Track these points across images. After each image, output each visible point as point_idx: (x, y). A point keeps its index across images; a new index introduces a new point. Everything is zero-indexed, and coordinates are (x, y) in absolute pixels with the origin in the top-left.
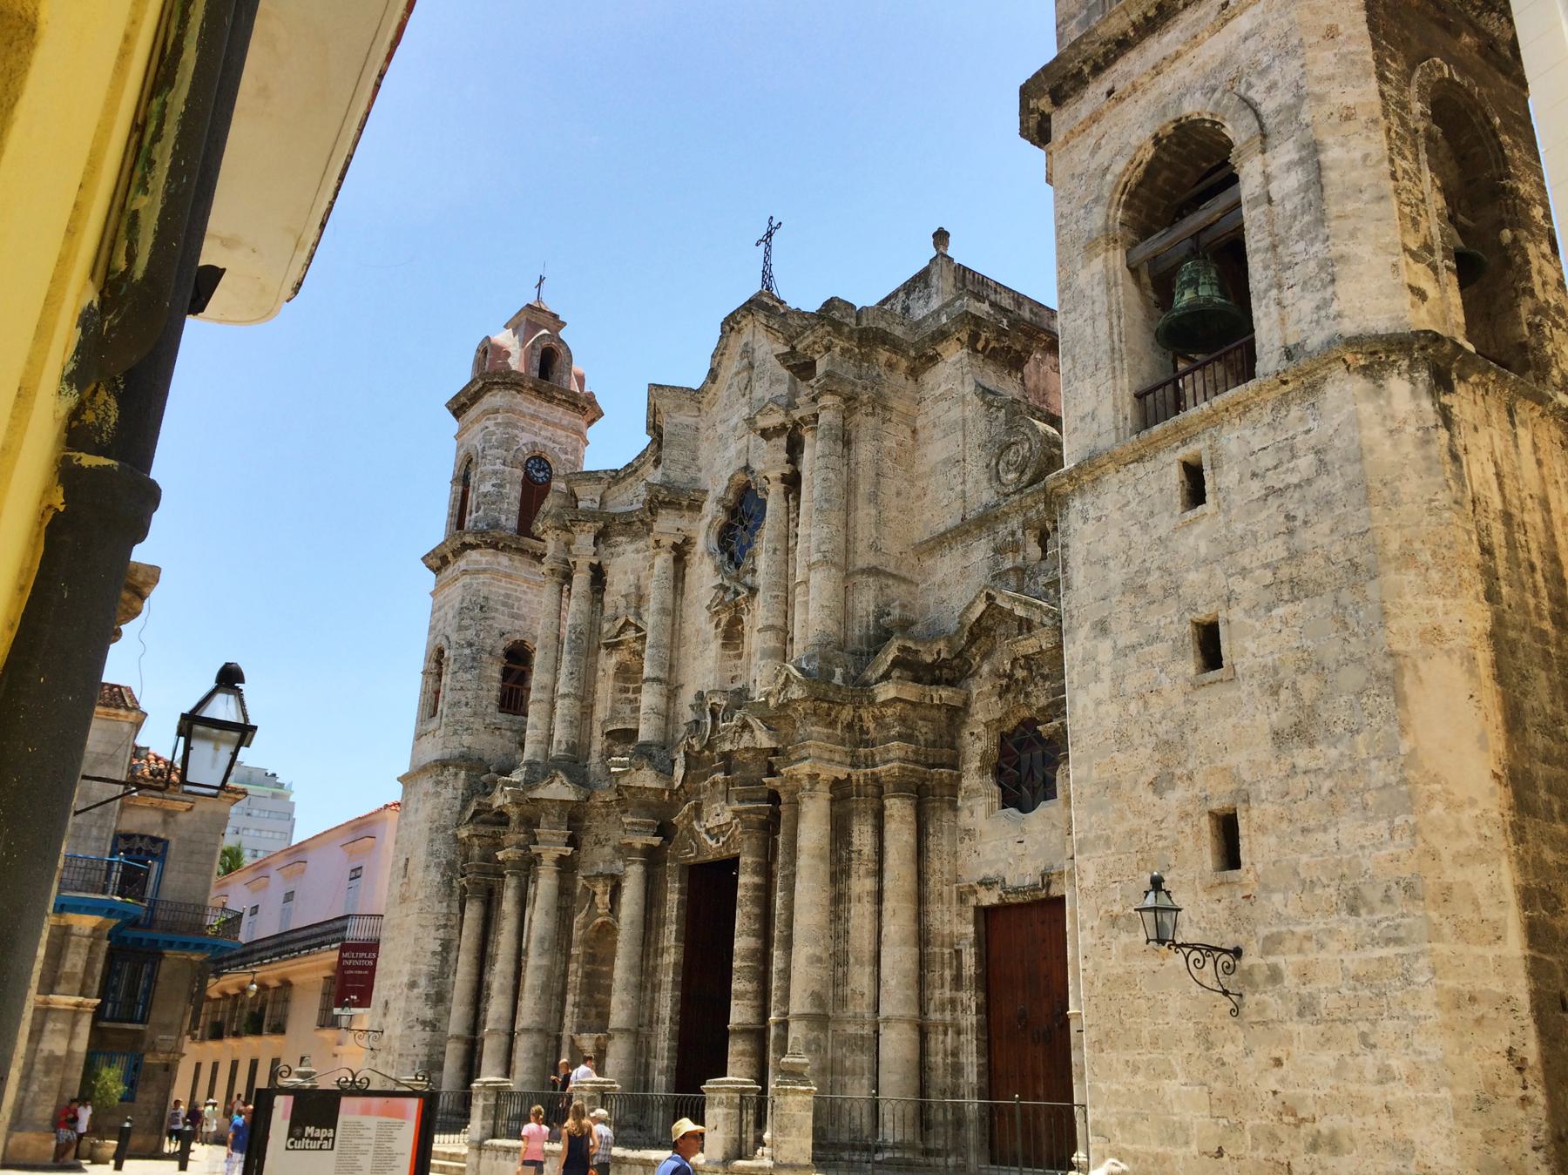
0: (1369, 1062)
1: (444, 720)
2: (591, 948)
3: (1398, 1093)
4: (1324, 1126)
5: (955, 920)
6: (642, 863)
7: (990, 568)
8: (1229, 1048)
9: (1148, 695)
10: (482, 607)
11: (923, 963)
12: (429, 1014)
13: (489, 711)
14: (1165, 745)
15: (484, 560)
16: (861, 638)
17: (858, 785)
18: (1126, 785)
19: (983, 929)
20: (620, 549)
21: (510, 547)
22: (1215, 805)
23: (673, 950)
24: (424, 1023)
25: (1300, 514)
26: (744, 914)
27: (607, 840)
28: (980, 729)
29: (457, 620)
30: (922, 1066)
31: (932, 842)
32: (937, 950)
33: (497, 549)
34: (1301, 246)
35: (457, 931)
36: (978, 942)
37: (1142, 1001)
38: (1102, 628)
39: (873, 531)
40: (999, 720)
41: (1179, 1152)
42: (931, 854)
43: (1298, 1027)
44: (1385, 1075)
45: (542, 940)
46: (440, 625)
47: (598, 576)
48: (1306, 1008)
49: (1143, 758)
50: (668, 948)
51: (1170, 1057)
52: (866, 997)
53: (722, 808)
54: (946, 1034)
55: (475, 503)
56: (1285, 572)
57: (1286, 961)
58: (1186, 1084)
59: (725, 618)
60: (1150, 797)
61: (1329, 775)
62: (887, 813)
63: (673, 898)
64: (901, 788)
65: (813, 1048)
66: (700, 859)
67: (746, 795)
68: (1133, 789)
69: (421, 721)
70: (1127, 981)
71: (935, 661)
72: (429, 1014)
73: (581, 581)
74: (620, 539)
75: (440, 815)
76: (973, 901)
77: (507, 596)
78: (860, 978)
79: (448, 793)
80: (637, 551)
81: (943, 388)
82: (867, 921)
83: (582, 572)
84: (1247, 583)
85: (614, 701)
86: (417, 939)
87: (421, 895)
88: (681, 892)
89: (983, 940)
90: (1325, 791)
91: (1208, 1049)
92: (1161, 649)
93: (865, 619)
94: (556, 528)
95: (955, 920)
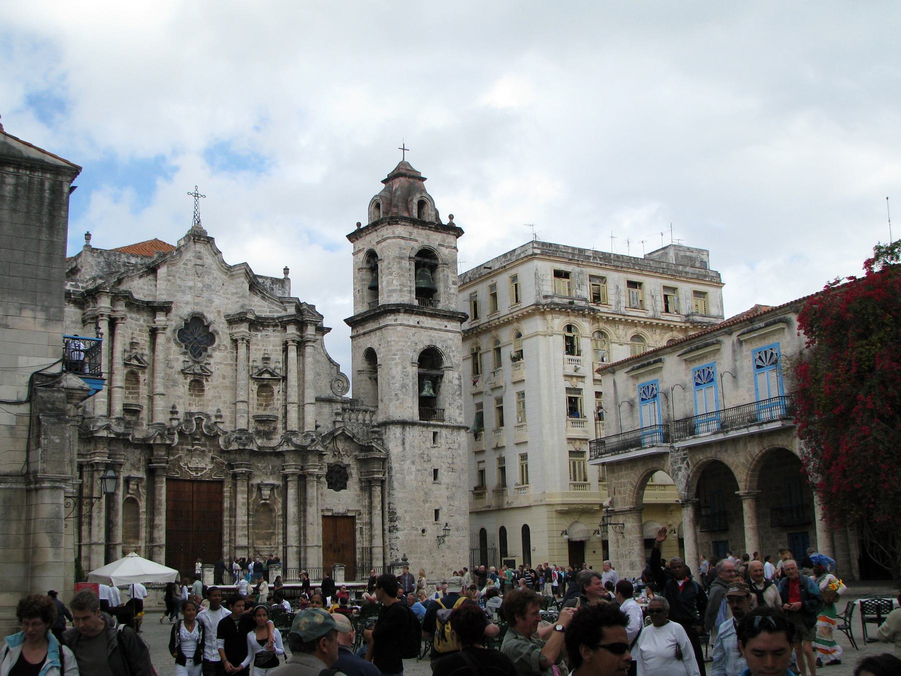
4: (450, 567)
14: (426, 493)
34: (457, 398)
43: (447, 550)
48: (449, 547)
53: (200, 461)
56: (452, 466)
70: (416, 541)
92: (426, 473)
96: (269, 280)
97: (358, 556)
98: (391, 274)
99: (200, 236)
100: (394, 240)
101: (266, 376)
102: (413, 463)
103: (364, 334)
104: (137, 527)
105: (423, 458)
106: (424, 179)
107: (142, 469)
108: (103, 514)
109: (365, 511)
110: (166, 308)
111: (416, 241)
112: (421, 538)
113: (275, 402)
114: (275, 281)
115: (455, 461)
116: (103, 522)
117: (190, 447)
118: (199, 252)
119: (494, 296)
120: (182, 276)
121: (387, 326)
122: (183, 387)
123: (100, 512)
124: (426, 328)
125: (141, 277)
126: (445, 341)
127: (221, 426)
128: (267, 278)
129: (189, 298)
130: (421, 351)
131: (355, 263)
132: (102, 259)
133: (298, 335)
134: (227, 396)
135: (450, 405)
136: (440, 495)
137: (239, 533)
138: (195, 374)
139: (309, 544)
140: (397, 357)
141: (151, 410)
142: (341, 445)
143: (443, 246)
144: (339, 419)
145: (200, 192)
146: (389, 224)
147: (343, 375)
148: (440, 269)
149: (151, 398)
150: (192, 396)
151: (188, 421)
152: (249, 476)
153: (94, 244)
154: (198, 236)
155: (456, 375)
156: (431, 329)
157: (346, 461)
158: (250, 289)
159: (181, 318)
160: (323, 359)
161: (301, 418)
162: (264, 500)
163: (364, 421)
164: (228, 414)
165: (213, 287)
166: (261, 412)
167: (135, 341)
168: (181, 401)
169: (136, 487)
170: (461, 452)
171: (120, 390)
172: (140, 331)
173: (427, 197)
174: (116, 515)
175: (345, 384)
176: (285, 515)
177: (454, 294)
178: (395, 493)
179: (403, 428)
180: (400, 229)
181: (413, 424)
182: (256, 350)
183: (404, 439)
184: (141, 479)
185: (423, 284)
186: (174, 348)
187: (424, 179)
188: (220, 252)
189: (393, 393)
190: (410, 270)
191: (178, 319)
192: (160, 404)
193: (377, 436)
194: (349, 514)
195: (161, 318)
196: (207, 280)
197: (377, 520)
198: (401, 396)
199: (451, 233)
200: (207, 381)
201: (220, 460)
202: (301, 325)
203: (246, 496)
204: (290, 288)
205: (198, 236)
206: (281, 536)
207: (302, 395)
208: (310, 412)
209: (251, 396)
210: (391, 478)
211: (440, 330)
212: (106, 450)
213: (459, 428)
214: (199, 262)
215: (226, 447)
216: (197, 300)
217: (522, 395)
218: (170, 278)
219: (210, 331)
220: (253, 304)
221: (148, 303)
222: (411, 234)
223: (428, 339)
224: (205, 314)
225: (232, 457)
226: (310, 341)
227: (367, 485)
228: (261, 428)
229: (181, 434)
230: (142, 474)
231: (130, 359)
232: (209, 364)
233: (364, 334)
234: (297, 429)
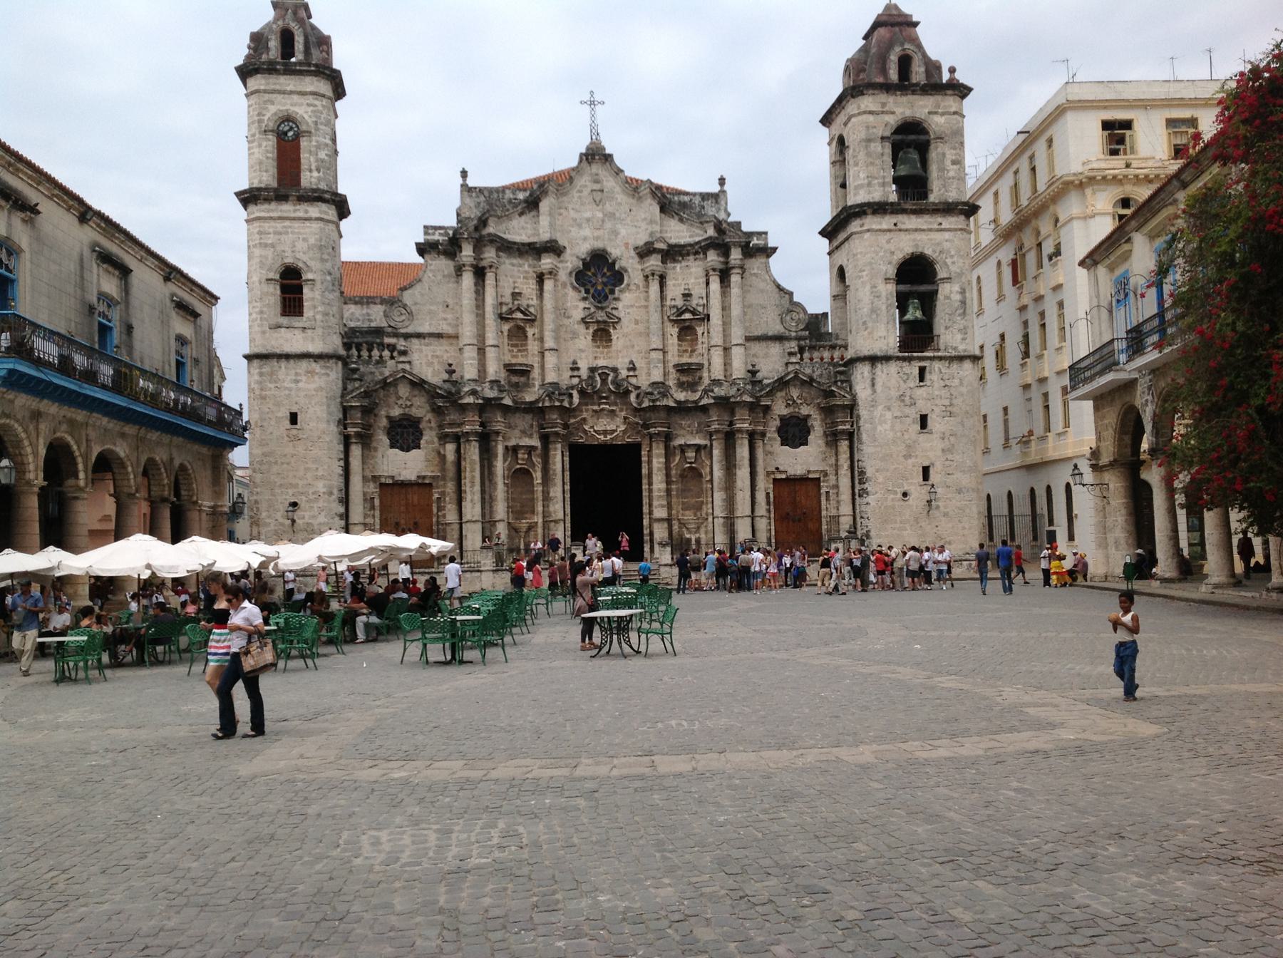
0: (960, 525)
3: (966, 532)
10: (333, 248)
14: (909, 446)
15: (330, 212)
18: (894, 456)
20: (502, 260)
25: (955, 394)
44: (964, 528)
48: (946, 515)
49: (902, 448)
56: (948, 409)
60: (902, 459)
63: (567, 459)
70: (893, 507)
72: (342, 510)
74: (501, 254)
80: (513, 265)
81: (755, 271)
92: (909, 420)
96: (697, 197)
97: (824, 527)
98: (856, 164)
99: (593, 155)
100: (860, 118)
101: (687, 316)
102: (889, 409)
103: (837, 248)
104: (532, 500)
105: (903, 401)
106: (916, 24)
107: (536, 436)
108: (477, 488)
109: (830, 471)
110: (553, 248)
111: (893, 113)
112: (902, 503)
113: (700, 346)
114: (705, 196)
115: (954, 402)
116: (477, 497)
117: (596, 408)
118: (597, 175)
119: (1033, 169)
120: (577, 207)
121: (852, 234)
122: (584, 339)
123: (472, 486)
124: (906, 230)
125: (521, 214)
126: (938, 244)
127: (633, 381)
128: (694, 194)
129: (587, 232)
130: (901, 261)
131: (831, 156)
132: (482, 198)
133: (723, 263)
134: (641, 344)
135: (946, 328)
136: (930, 448)
137: (655, 503)
138: (598, 322)
139: (738, 513)
140: (864, 273)
141: (543, 367)
142: (795, 393)
143: (936, 113)
144: (794, 360)
145: (597, 98)
146: (853, 97)
147: (798, 305)
148: (932, 147)
149: (542, 354)
150: (598, 347)
151: (589, 377)
152: (668, 437)
153: (471, 182)
154: (596, 155)
155: (956, 288)
156: (916, 230)
157: (805, 410)
158: (663, 210)
159: (577, 257)
160: (771, 287)
161: (727, 364)
162: (691, 463)
163: (832, 358)
164: (643, 365)
165: (617, 215)
166: (685, 360)
167: (517, 291)
168: (583, 355)
169: (526, 456)
170: (964, 390)
171: (493, 349)
172: (524, 278)
173: (912, 48)
174: (495, 489)
175: (802, 315)
176: (711, 481)
177: (953, 178)
178: (864, 447)
179: (873, 365)
180: (868, 102)
181: (887, 359)
182: (674, 285)
183: (873, 379)
184: (532, 448)
185: (903, 170)
186: (571, 293)
187: (916, 24)
188: (622, 171)
189: (861, 322)
190: (882, 155)
191: (575, 259)
192: (551, 359)
193: (842, 378)
194: (811, 476)
195: (547, 262)
196: (609, 207)
197: (845, 482)
198: (870, 325)
199: (949, 92)
200: (615, 328)
201: (632, 419)
202: (724, 250)
203: (663, 460)
204: (726, 204)
205: (596, 155)
206: (710, 506)
207: (726, 334)
208: (738, 356)
209: (670, 342)
210: (859, 430)
211: (930, 230)
212: (476, 418)
213: (961, 358)
214: (597, 187)
215: (640, 404)
216: (597, 233)
217: (1061, 305)
218: (562, 211)
219: (617, 267)
220: (669, 229)
221: (530, 244)
222: (884, 105)
223: (911, 243)
224: (609, 249)
225: (648, 415)
226: (733, 268)
227: (832, 438)
228: (684, 379)
229: (582, 393)
230: (536, 442)
231: (511, 312)
232: (616, 309)
233: (837, 248)
234: (722, 377)
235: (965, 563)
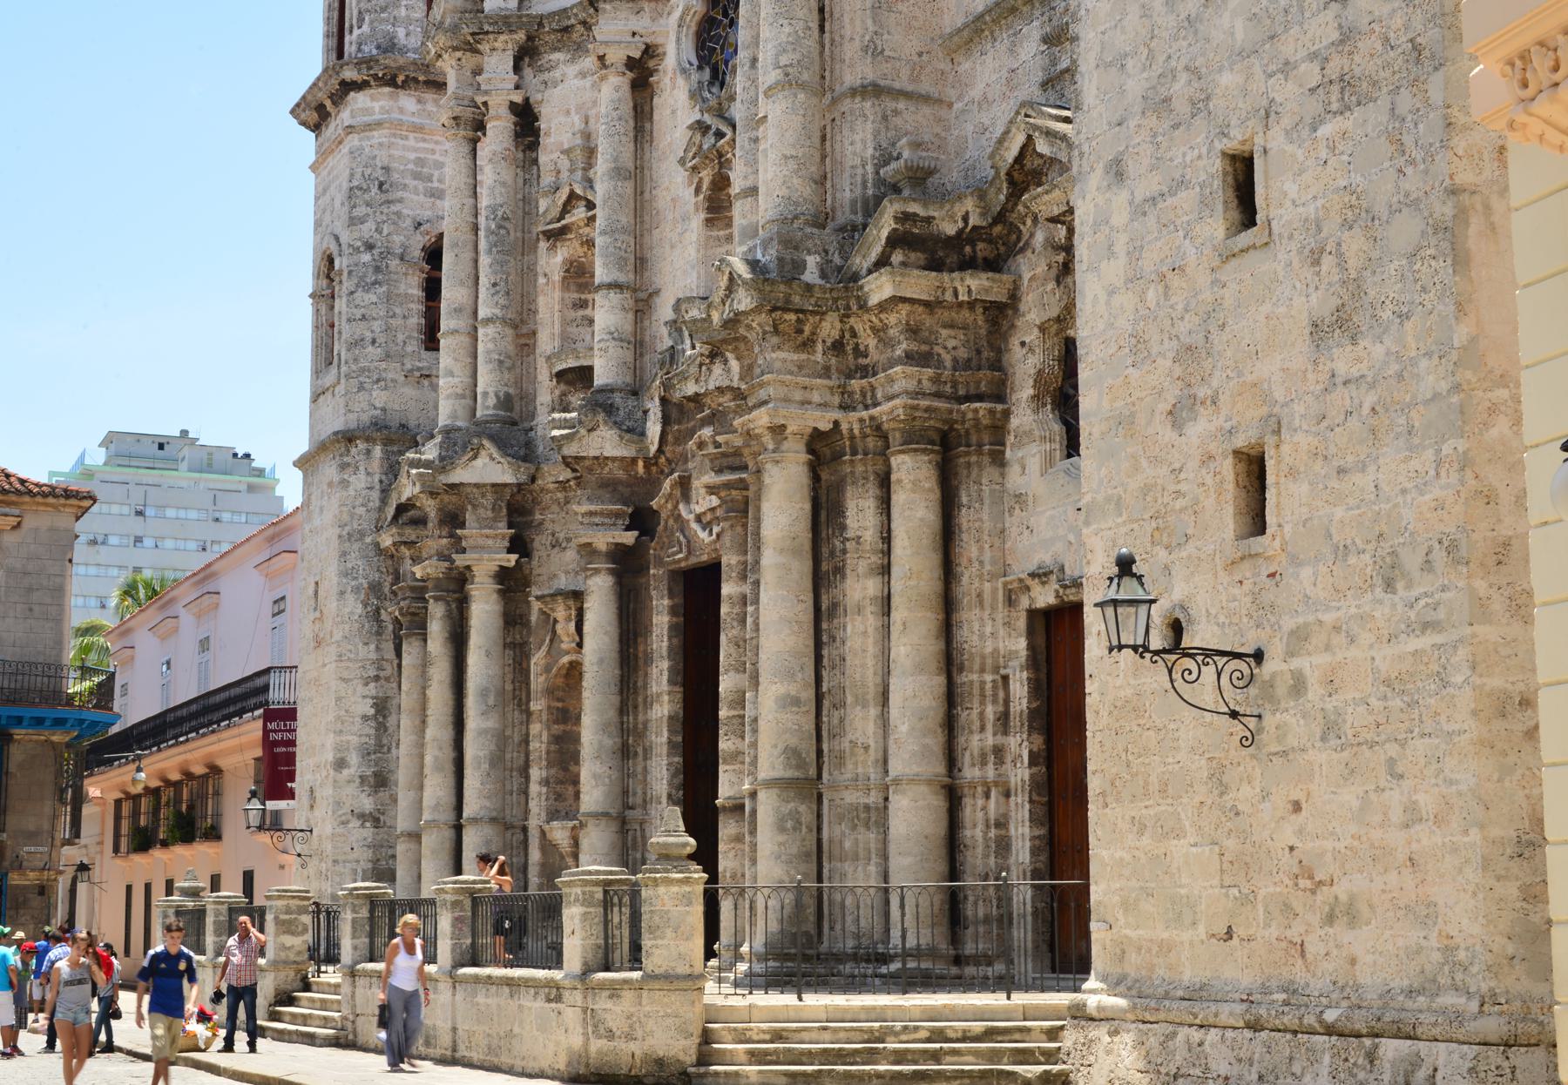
0: (1395, 798)
1: (344, 369)
2: (559, 700)
4: (1341, 890)
5: (1002, 632)
6: (611, 572)
7: (1044, 69)
8: (1246, 790)
9: (1170, 275)
10: (381, 185)
11: (952, 698)
12: (367, 804)
13: (409, 349)
15: (377, 105)
16: (853, 202)
17: (852, 438)
19: (1041, 641)
20: (557, 74)
21: (415, 80)
22: (1240, 442)
23: (666, 698)
24: (363, 817)
26: (730, 641)
27: (569, 540)
28: (1032, 336)
29: (346, 208)
30: (953, 843)
31: (965, 518)
32: (975, 677)
33: (396, 86)
35: (395, 685)
36: (1033, 662)
37: (1151, 733)
38: (1117, 172)
39: (869, 22)
40: (1058, 320)
41: (1186, 936)
42: (965, 536)
43: (1320, 757)
45: (484, 693)
46: (327, 219)
47: (526, 120)
48: (1330, 729)
50: (659, 695)
51: (1180, 809)
52: (872, 751)
54: (987, 796)
55: (355, 13)
56: (1335, 67)
57: (1311, 664)
58: (1195, 845)
59: (707, 175)
60: (1168, 434)
61: (1372, 386)
62: (894, 477)
64: (914, 438)
65: (789, 824)
66: (693, 560)
67: (725, 462)
68: (1149, 423)
69: (317, 373)
71: (960, 232)
72: (367, 804)
73: (499, 130)
75: (352, 515)
76: (1025, 603)
77: (420, 162)
78: (861, 724)
79: (359, 481)
80: (583, 75)
82: (871, 640)
83: (498, 118)
84: (1290, 86)
85: (565, 323)
86: (338, 699)
87: (338, 636)
88: (673, 611)
89: (1042, 657)
90: (1366, 410)
91: (1222, 794)
93: (860, 171)
94: (455, 49)
95: (1002, 632)
235: (1391, 1049)
